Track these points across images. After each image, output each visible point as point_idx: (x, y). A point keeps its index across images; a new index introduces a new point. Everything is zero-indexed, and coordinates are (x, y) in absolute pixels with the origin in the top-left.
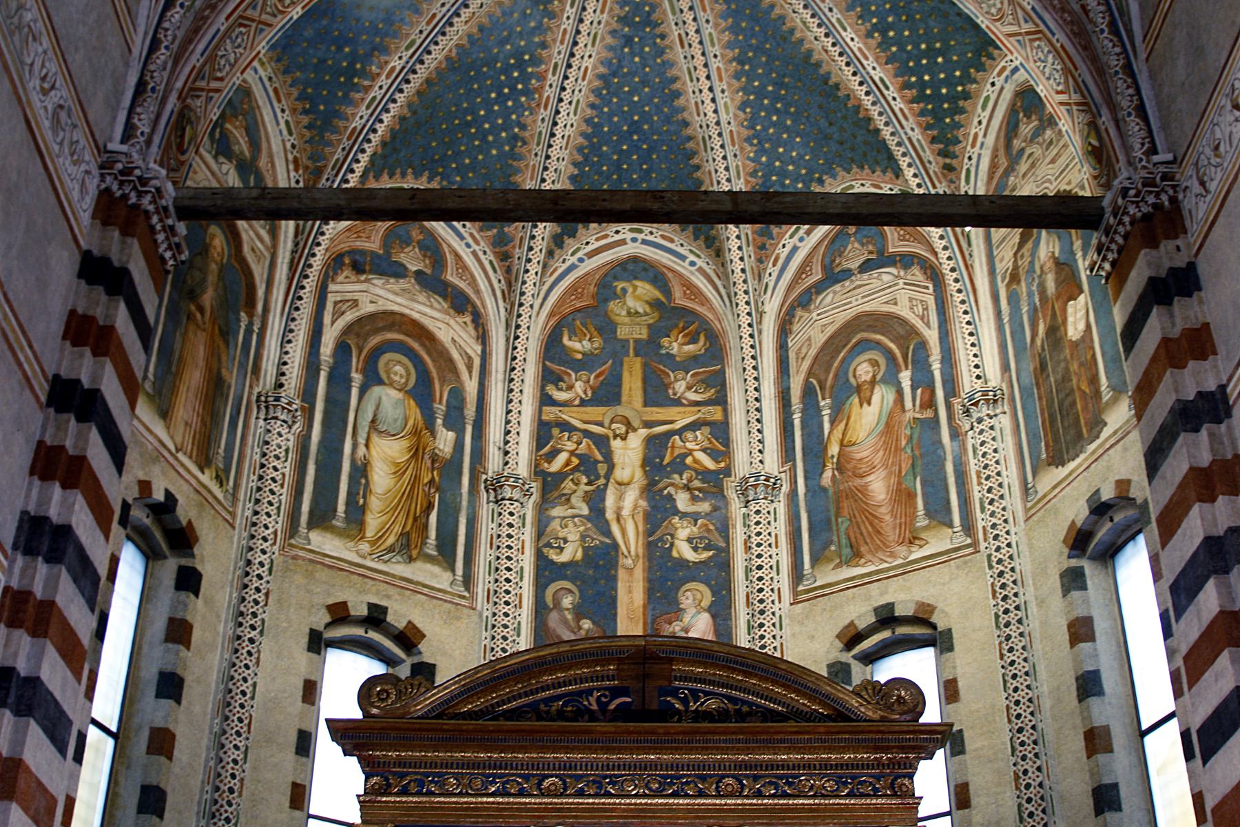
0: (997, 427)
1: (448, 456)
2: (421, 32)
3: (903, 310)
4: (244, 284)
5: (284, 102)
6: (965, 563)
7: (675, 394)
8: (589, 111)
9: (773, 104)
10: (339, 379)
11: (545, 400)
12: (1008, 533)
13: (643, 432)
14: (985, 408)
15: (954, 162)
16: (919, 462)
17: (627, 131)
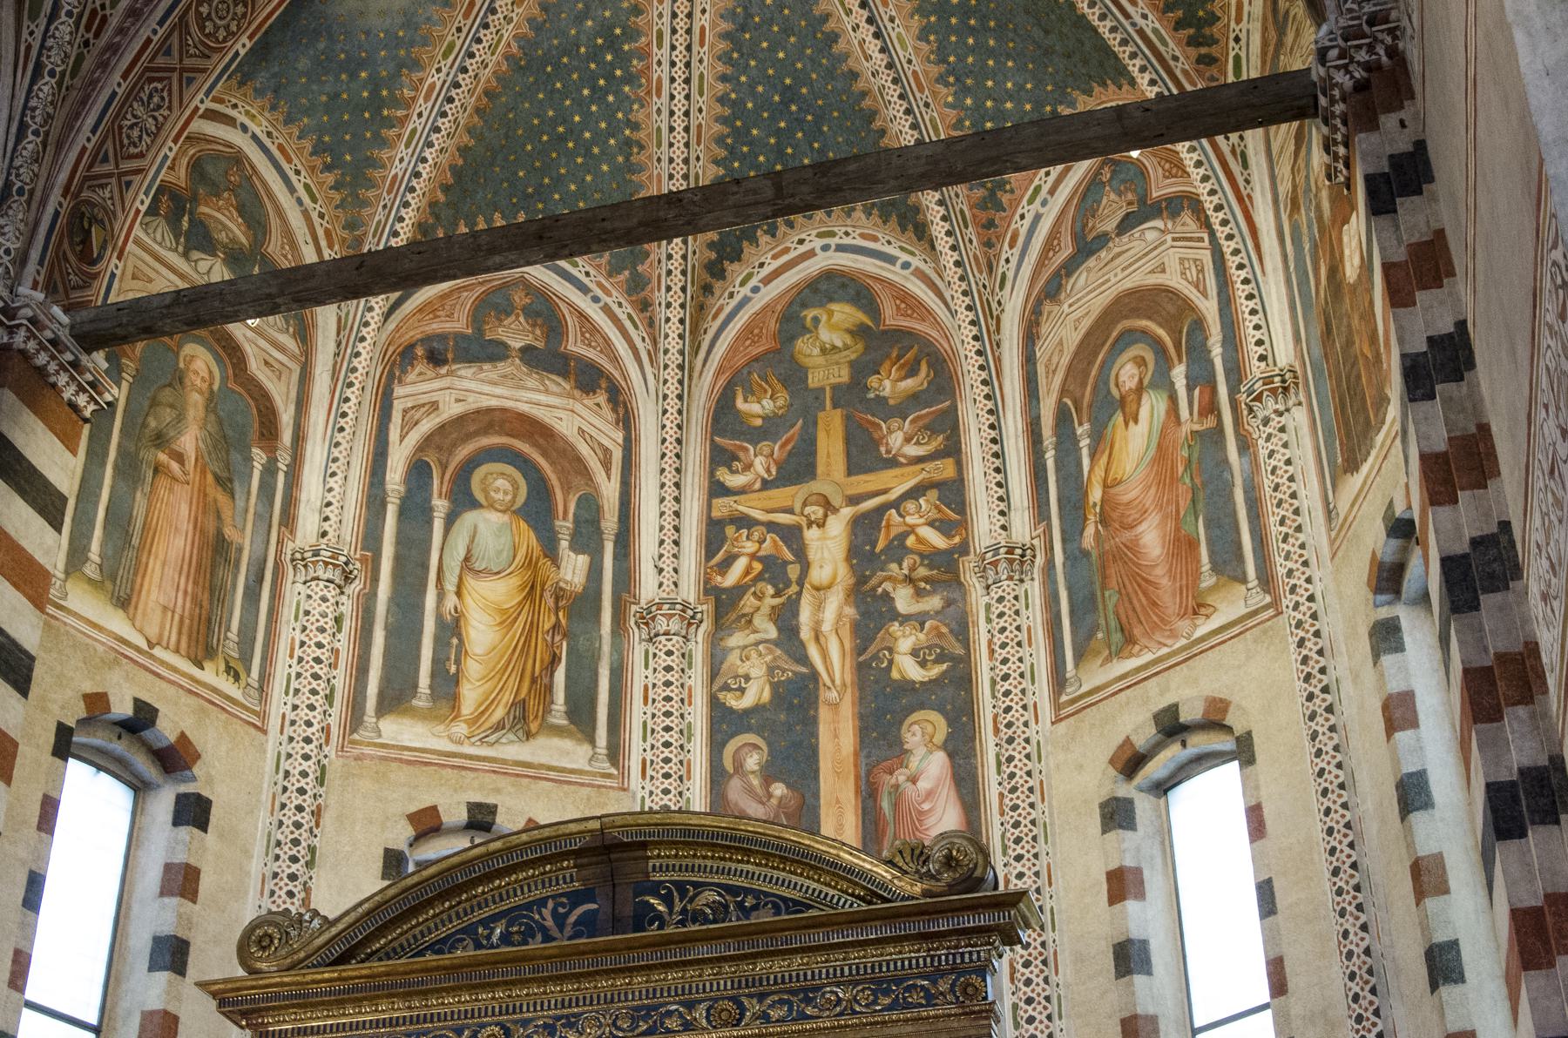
0: (1290, 427)
1: (580, 589)
2: (459, 30)
3: (1173, 280)
4: (255, 411)
5: (296, 161)
6: (1265, 632)
7: (888, 452)
8: (721, 87)
9: (963, 22)
10: (415, 510)
11: (717, 489)
12: (1308, 580)
13: (847, 512)
15: (1214, 51)
16: (1201, 495)
17: (781, 102)
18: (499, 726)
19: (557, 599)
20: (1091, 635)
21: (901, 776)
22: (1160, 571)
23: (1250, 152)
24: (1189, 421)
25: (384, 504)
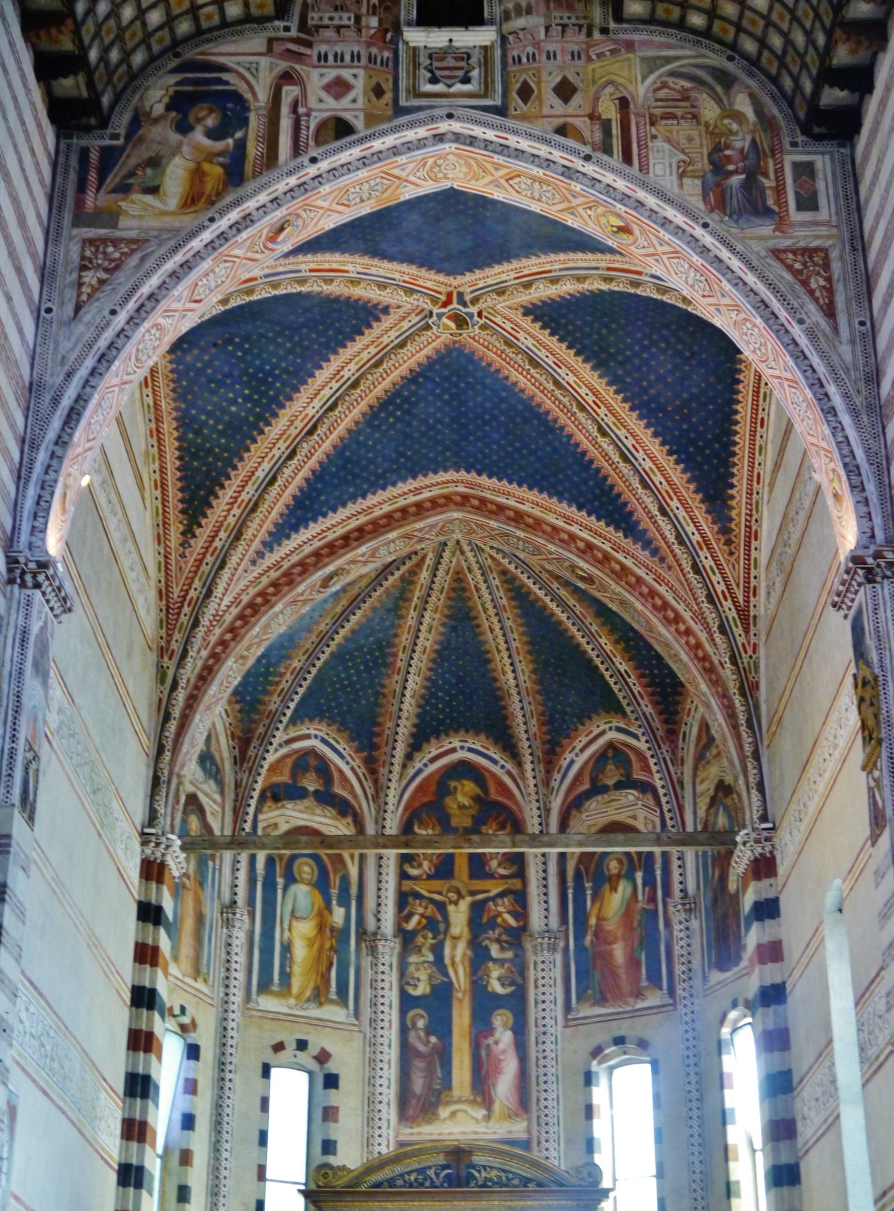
0: (692, 927)
8: (428, 673)
10: (270, 886)
11: (403, 876)
13: (469, 899)
14: (683, 915)
15: (675, 727)
18: (308, 1000)
20: (587, 988)
21: (491, 1041)
23: (685, 782)
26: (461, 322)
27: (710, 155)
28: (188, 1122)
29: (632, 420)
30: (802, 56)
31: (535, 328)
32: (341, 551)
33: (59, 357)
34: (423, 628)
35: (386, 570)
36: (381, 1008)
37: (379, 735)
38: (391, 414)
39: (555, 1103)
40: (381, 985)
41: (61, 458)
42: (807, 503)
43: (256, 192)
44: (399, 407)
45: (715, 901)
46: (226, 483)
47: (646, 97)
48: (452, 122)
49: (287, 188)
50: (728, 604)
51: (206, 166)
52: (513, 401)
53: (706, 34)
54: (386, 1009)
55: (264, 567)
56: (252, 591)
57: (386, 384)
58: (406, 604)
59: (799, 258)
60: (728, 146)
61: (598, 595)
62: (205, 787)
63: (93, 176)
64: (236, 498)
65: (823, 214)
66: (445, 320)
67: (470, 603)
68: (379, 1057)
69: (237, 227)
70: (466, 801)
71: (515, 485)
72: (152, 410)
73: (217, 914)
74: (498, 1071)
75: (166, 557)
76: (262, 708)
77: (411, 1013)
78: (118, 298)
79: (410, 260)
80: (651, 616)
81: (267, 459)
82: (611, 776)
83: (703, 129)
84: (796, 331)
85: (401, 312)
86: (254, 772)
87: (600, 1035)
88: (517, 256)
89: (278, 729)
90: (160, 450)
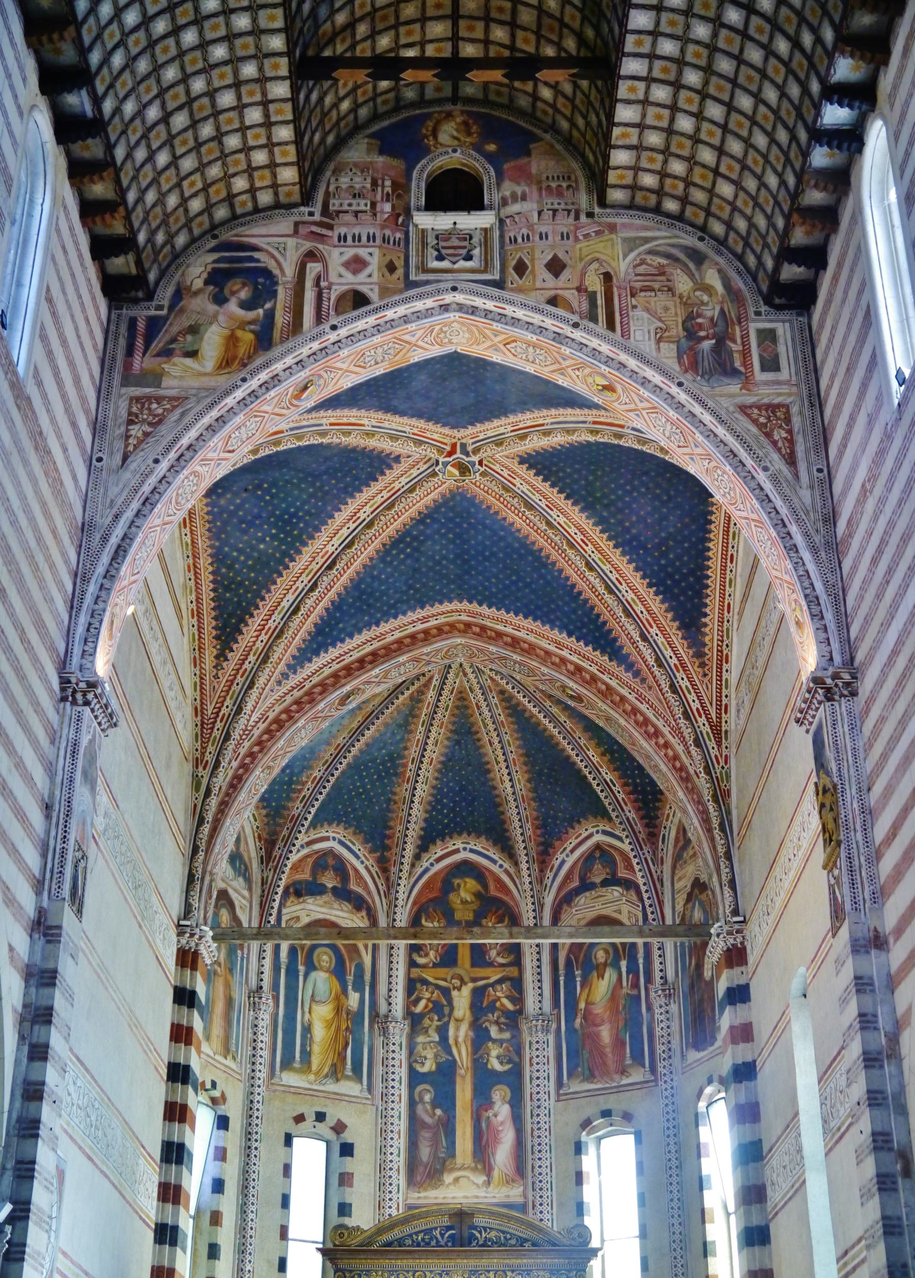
8: (434, 782)
10: (292, 972)
11: (412, 964)
13: (471, 985)
15: (656, 831)
18: (326, 1076)
19: (348, 1014)
20: (577, 1066)
21: (490, 1113)
22: (608, 1050)
24: (626, 989)
25: (280, 969)
26: (464, 469)
27: (684, 322)
28: (218, 1186)
29: (616, 556)
30: (764, 237)
31: (530, 475)
32: (357, 673)
33: (109, 500)
34: (430, 742)
35: (397, 690)
36: (392, 1084)
37: (390, 837)
38: (402, 551)
39: (548, 1170)
40: (391, 1062)
41: (109, 590)
42: (772, 630)
43: (283, 356)
44: (408, 545)
45: (692, 986)
46: (255, 613)
47: (627, 273)
48: (455, 294)
49: (310, 352)
50: (702, 720)
51: (239, 333)
52: (510, 540)
53: (679, 217)
54: (396, 1084)
55: (288, 687)
56: (278, 709)
57: (397, 524)
58: (415, 720)
59: (764, 412)
60: (699, 315)
61: (586, 712)
62: (235, 884)
63: (140, 342)
64: (264, 625)
65: (784, 375)
66: (449, 468)
67: (472, 719)
68: (390, 1128)
69: (266, 386)
70: (469, 898)
71: (512, 614)
72: (190, 547)
73: (244, 998)
74: (496, 1141)
75: (201, 678)
76: (286, 813)
77: (419, 1088)
78: (160, 449)
79: (419, 415)
80: (633, 731)
81: (291, 591)
82: (598, 874)
83: (678, 300)
84: (762, 477)
85: (411, 460)
86: (278, 870)
87: (589, 1108)
88: (514, 412)
89: (300, 832)
90: (197, 583)
